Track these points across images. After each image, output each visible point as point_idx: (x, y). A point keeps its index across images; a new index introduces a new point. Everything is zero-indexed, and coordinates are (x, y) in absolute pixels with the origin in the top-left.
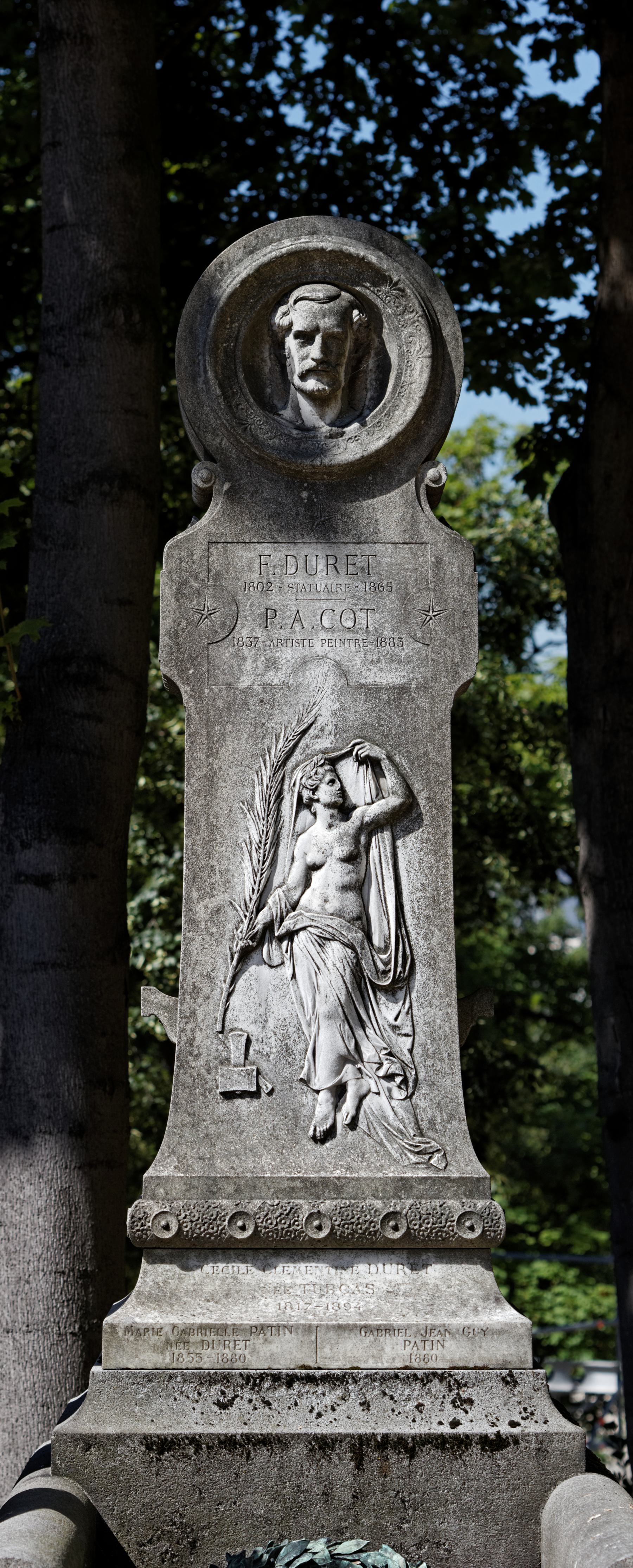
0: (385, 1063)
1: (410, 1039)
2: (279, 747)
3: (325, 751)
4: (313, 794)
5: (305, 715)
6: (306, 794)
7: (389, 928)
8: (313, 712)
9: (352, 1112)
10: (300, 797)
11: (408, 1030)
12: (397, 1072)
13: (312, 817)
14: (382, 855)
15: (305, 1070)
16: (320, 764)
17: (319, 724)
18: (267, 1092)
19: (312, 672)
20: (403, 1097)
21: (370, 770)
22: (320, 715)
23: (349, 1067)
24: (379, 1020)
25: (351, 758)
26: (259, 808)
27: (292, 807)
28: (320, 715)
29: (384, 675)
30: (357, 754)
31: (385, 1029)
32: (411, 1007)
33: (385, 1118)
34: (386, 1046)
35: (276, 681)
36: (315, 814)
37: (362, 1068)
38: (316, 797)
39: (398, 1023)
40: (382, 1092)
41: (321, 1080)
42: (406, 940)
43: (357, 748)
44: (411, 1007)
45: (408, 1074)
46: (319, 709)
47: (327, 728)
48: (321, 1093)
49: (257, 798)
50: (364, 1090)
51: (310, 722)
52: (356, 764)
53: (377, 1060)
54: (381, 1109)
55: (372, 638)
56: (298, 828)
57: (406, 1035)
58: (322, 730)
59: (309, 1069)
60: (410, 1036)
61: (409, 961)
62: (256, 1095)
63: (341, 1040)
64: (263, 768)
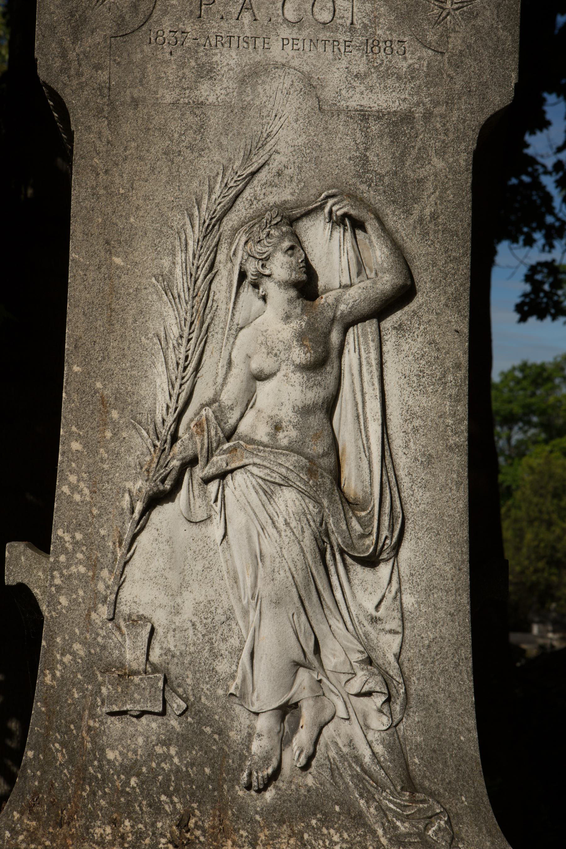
0: (360, 673)
1: (398, 638)
2: (214, 197)
3: (281, 208)
4: (263, 266)
5: (254, 152)
6: (252, 267)
7: (371, 471)
8: (268, 147)
9: (308, 749)
10: (243, 276)
11: (395, 624)
12: (378, 689)
13: (261, 302)
14: (364, 363)
15: (238, 680)
16: (274, 222)
17: (274, 166)
18: (178, 713)
19: (267, 87)
20: (385, 728)
21: (349, 234)
22: (277, 152)
23: (303, 676)
24: (352, 609)
25: (322, 217)
26: (180, 285)
27: (231, 285)
28: (277, 152)
29: (374, 97)
30: (331, 212)
31: (360, 623)
32: (399, 590)
33: (358, 759)
34: (362, 649)
35: (212, 99)
36: (264, 298)
37: (325, 680)
38: (267, 272)
39: (382, 612)
40: (353, 717)
41: (262, 697)
42: (395, 489)
43: (331, 202)
44: (399, 590)
45: (394, 692)
46: (276, 143)
47: (287, 172)
48: (260, 715)
49: (178, 271)
50: (327, 715)
51: (261, 161)
52: (329, 226)
53: (347, 668)
54: (351, 743)
55: (359, 40)
56: (239, 318)
57: (393, 632)
58: (279, 174)
59: (244, 680)
60: (397, 633)
61: (400, 520)
62: (163, 713)
63: (295, 637)
64: (189, 226)
